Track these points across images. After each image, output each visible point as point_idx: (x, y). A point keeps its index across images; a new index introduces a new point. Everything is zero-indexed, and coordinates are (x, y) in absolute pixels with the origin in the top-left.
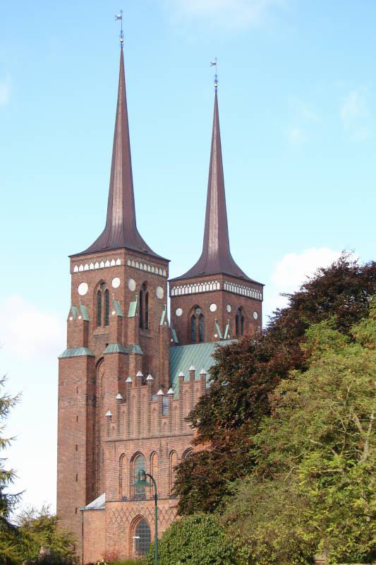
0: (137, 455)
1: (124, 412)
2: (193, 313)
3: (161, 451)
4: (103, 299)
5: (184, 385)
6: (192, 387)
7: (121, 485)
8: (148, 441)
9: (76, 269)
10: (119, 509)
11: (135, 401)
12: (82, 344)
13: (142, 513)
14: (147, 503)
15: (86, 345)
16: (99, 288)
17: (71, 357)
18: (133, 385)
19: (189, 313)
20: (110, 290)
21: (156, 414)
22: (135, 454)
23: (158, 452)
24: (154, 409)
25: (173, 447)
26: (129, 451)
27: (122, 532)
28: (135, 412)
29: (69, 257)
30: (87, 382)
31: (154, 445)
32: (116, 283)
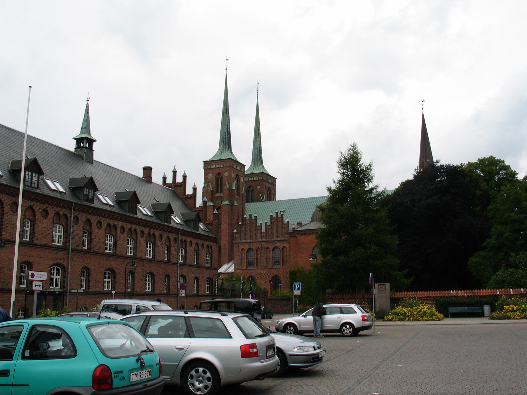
0: (250, 249)
1: (243, 230)
2: (249, 189)
3: (262, 247)
4: (219, 181)
5: (273, 219)
7: (241, 263)
8: (255, 243)
10: (241, 273)
11: (248, 225)
12: (210, 200)
13: (252, 275)
19: (247, 189)
20: (224, 177)
25: (268, 246)
26: (246, 247)
28: (248, 230)
29: (203, 162)
30: (213, 217)
32: (226, 174)
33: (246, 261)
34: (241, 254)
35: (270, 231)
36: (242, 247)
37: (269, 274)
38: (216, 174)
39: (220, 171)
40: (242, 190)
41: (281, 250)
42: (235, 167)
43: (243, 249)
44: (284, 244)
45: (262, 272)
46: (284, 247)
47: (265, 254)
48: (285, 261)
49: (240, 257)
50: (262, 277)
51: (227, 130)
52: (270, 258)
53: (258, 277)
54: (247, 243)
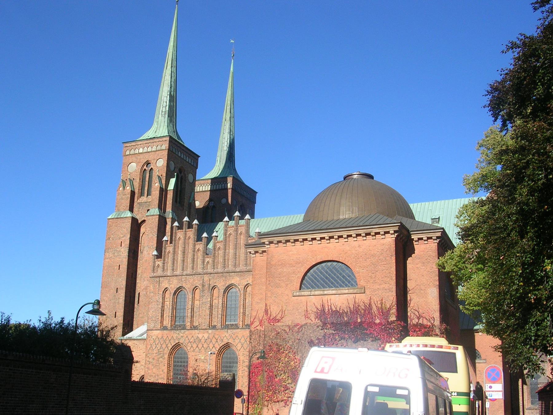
0: (178, 290)
1: (169, 252)
5: (229, 229)
6: (237, 230)
7: (162, 316)
10: (160, 336)
11: (181, 242)
13: (181, 341)
14: (187, 332)
15: (131, 209)
16: (145, 167)
17: (117, 218)
18: (169, 242)
21: (200, 254)
22: (178, 289)
23: (200, 287)
24: (198, 250)
25: (215, 283)
27: (161, 357)
28: (179, 252)
31: (197, 281)
33: (170, 314)
34: (164, 298)
35: (221, 252)
36: (165, 284)
37: (214, 341)
38: (143, 164)
40: (190, 197)
41: (242, 292)
42: (177, 153)
43: (166, 290)
44: (248, 279)
45: (200, 336)
46: (247, 286)
47: (209, 300)
48: (248, 315)
49: (161, 304)
50: (200, 346)
51: (169, 93)
52: (218, 309)
53: (192, 346)
54: (175, 278)
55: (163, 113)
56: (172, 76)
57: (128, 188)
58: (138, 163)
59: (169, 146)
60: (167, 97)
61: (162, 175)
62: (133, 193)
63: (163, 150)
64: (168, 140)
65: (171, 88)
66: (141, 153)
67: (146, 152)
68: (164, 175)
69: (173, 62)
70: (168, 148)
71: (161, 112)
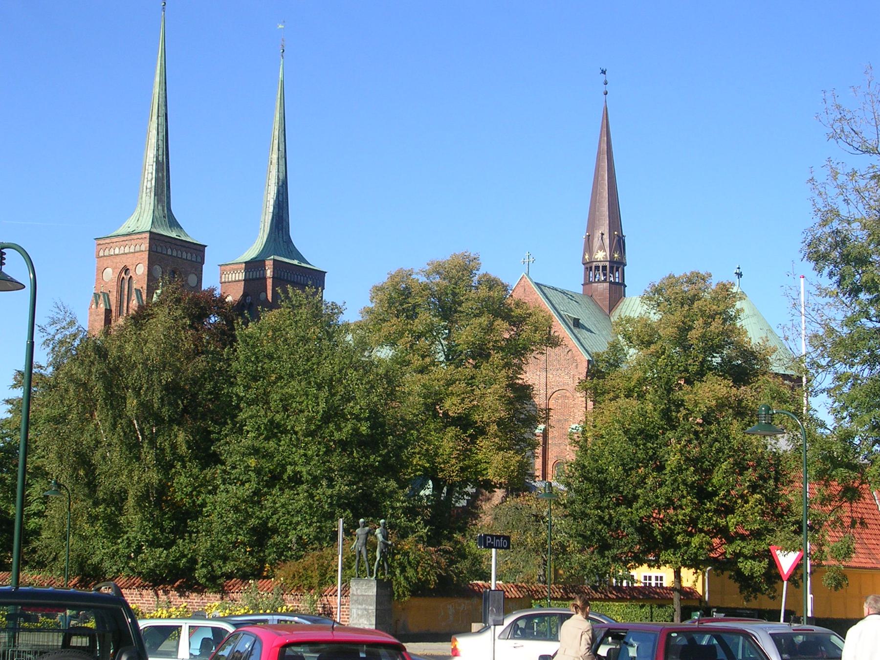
9: (101, 254)
16: (123, 275)
39: (128, 262)
55: (148, 190)
56: (159, 130)
57: (102, 306)
58: (114, 269)
59: (149, 246)
60: (152, 165)
61: (142, 288)
62: (108, 312)
63: (143, 251)
64: (148, 238)
65: (158, 150)
66: (117, 255)
67: (123, 254)
68: (145, 286)
69: (160, 109)
70: (148, 249)
71: (145, 188)
